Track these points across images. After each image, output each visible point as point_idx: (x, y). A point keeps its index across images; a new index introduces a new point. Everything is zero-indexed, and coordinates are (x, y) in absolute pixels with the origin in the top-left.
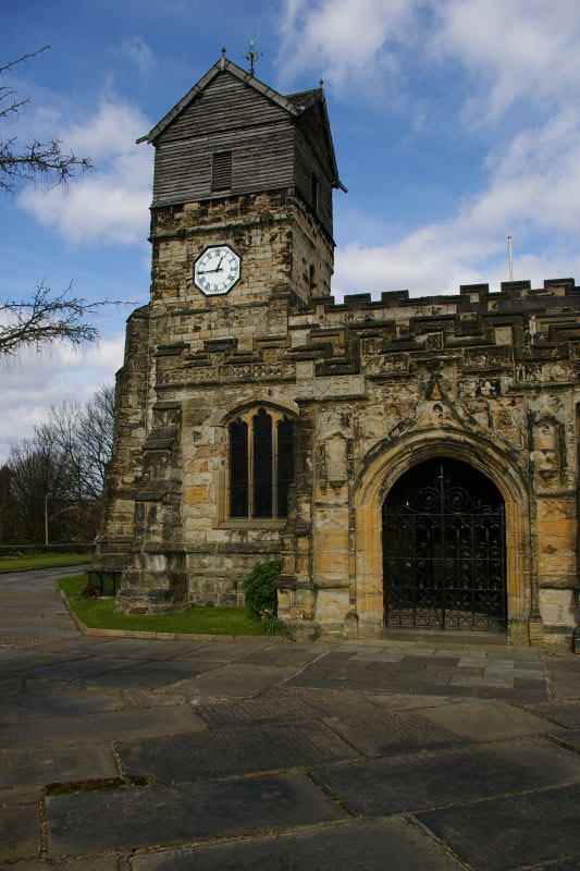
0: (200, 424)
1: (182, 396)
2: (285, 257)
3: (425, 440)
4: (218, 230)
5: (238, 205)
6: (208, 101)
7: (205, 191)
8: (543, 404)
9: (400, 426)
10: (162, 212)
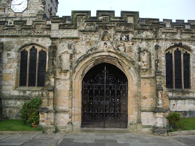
0: (10, 50)
2: (43, 2)
3: (100, 56)
8: (144, 45)
9: (91, 50)
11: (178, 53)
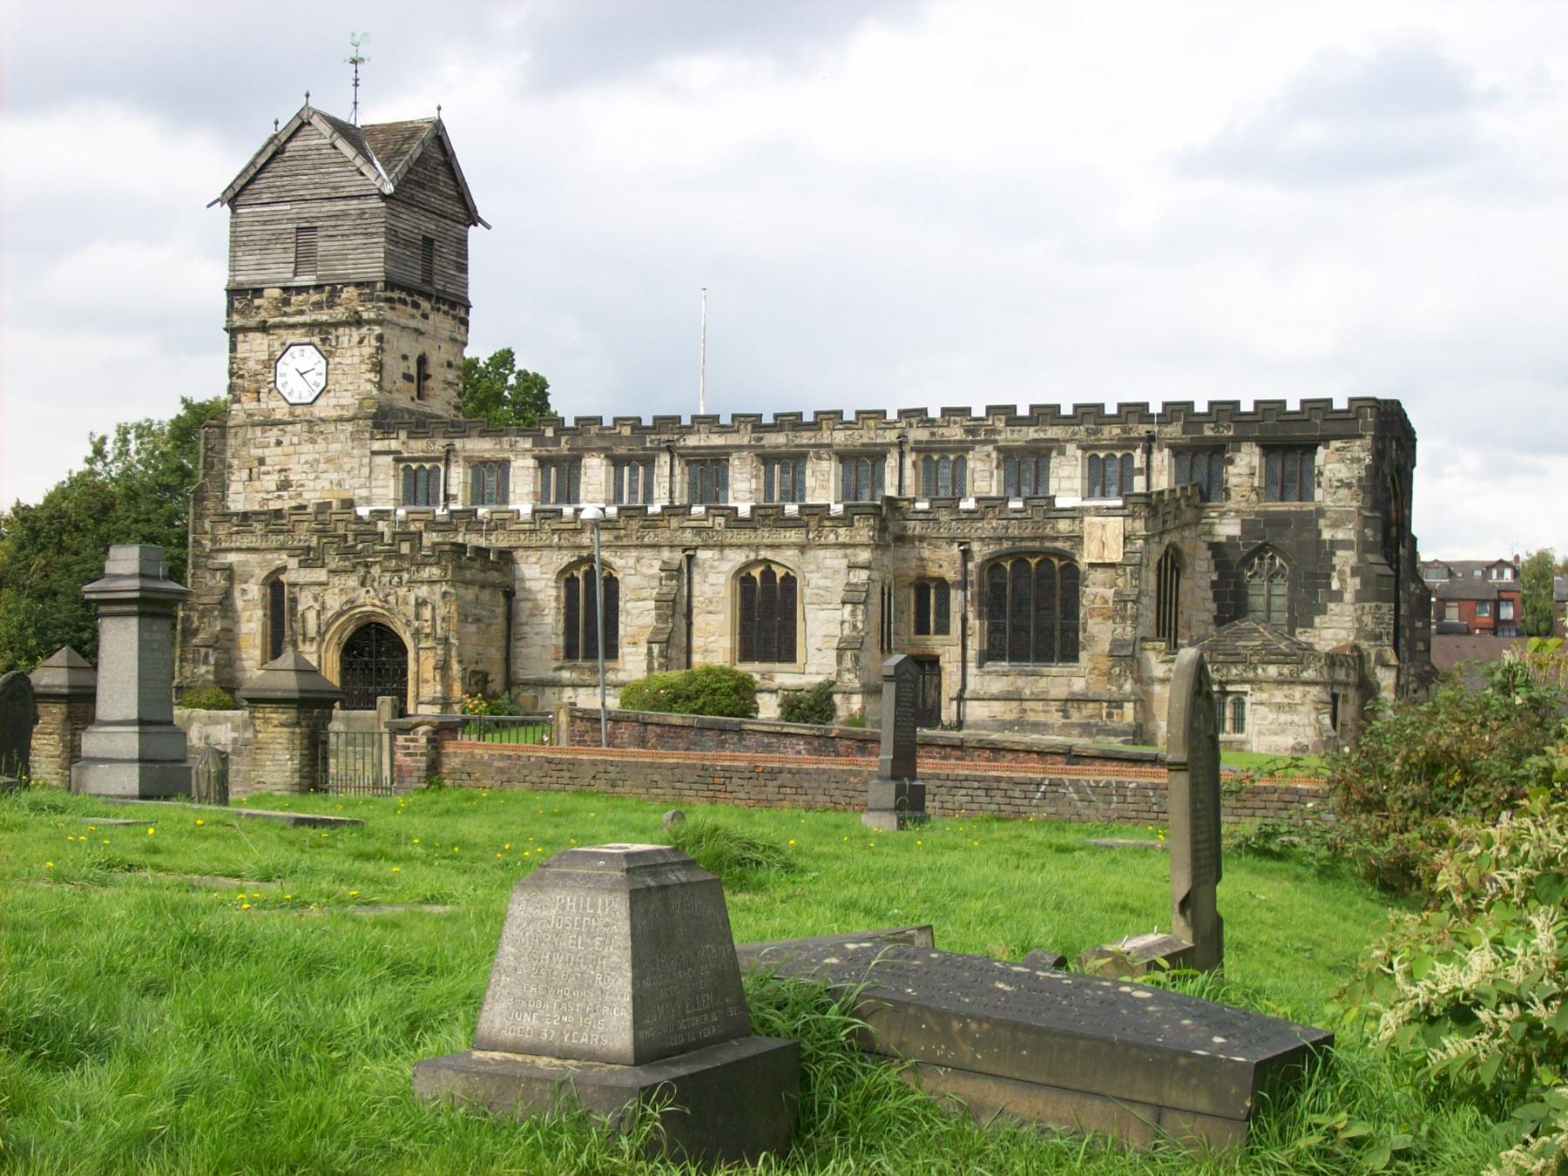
1: (232, 558)
2: (374, 364)
4: (304, 325)
5: (324, 296)
6: (292, 158)
7: (286, 274)
8: (423, 591)
10: (239, 295)
11: (590, 575)
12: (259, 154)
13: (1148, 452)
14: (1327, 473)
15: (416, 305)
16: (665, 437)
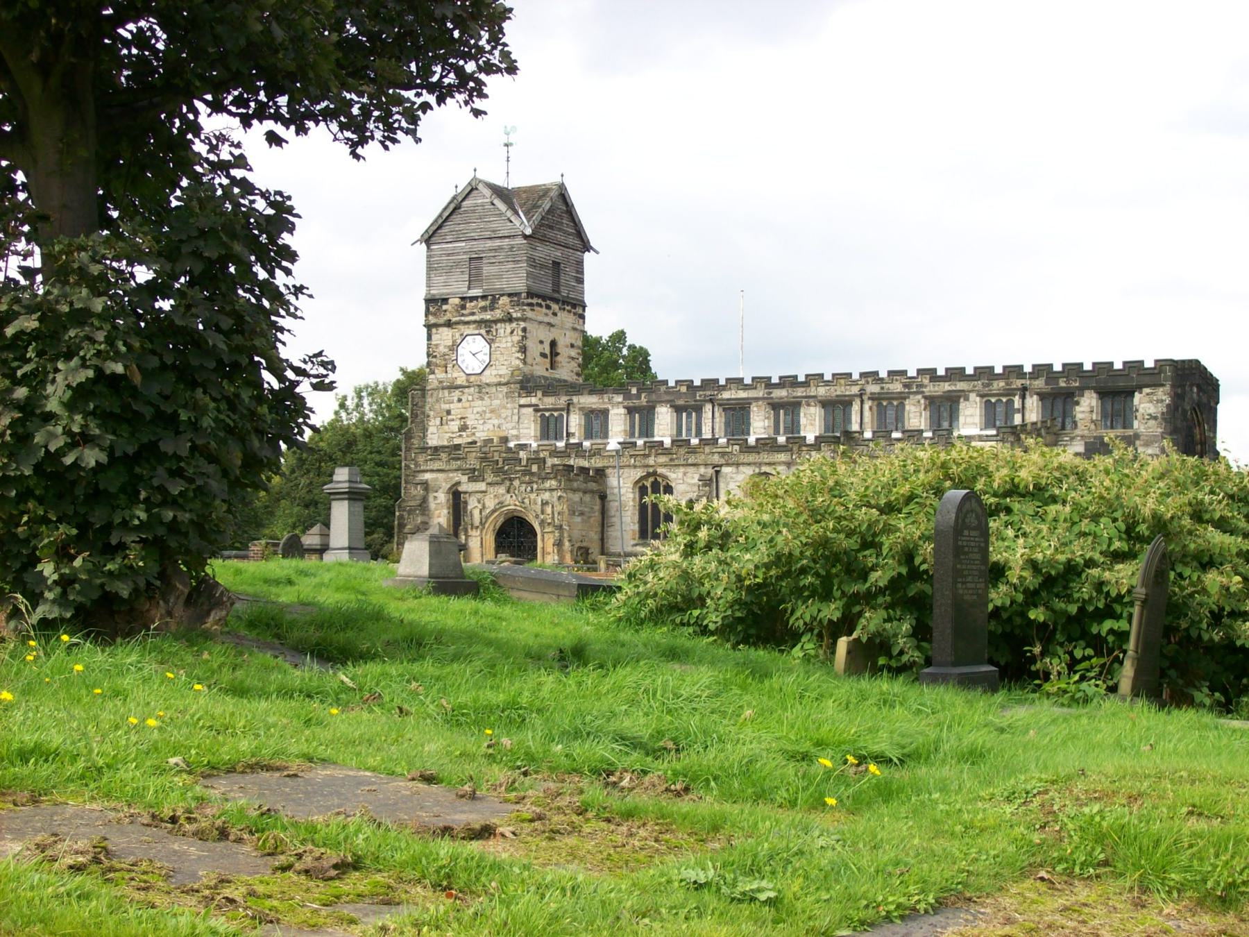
1: (428, 476)
4: (475, 322)
5: (488, 303)
8: (546, 496)
10: (434, 303)
12: (445, 209)
13: (1023, 398)
14: (1141, 410)
15: (548, 307)
16: (708, 393)
